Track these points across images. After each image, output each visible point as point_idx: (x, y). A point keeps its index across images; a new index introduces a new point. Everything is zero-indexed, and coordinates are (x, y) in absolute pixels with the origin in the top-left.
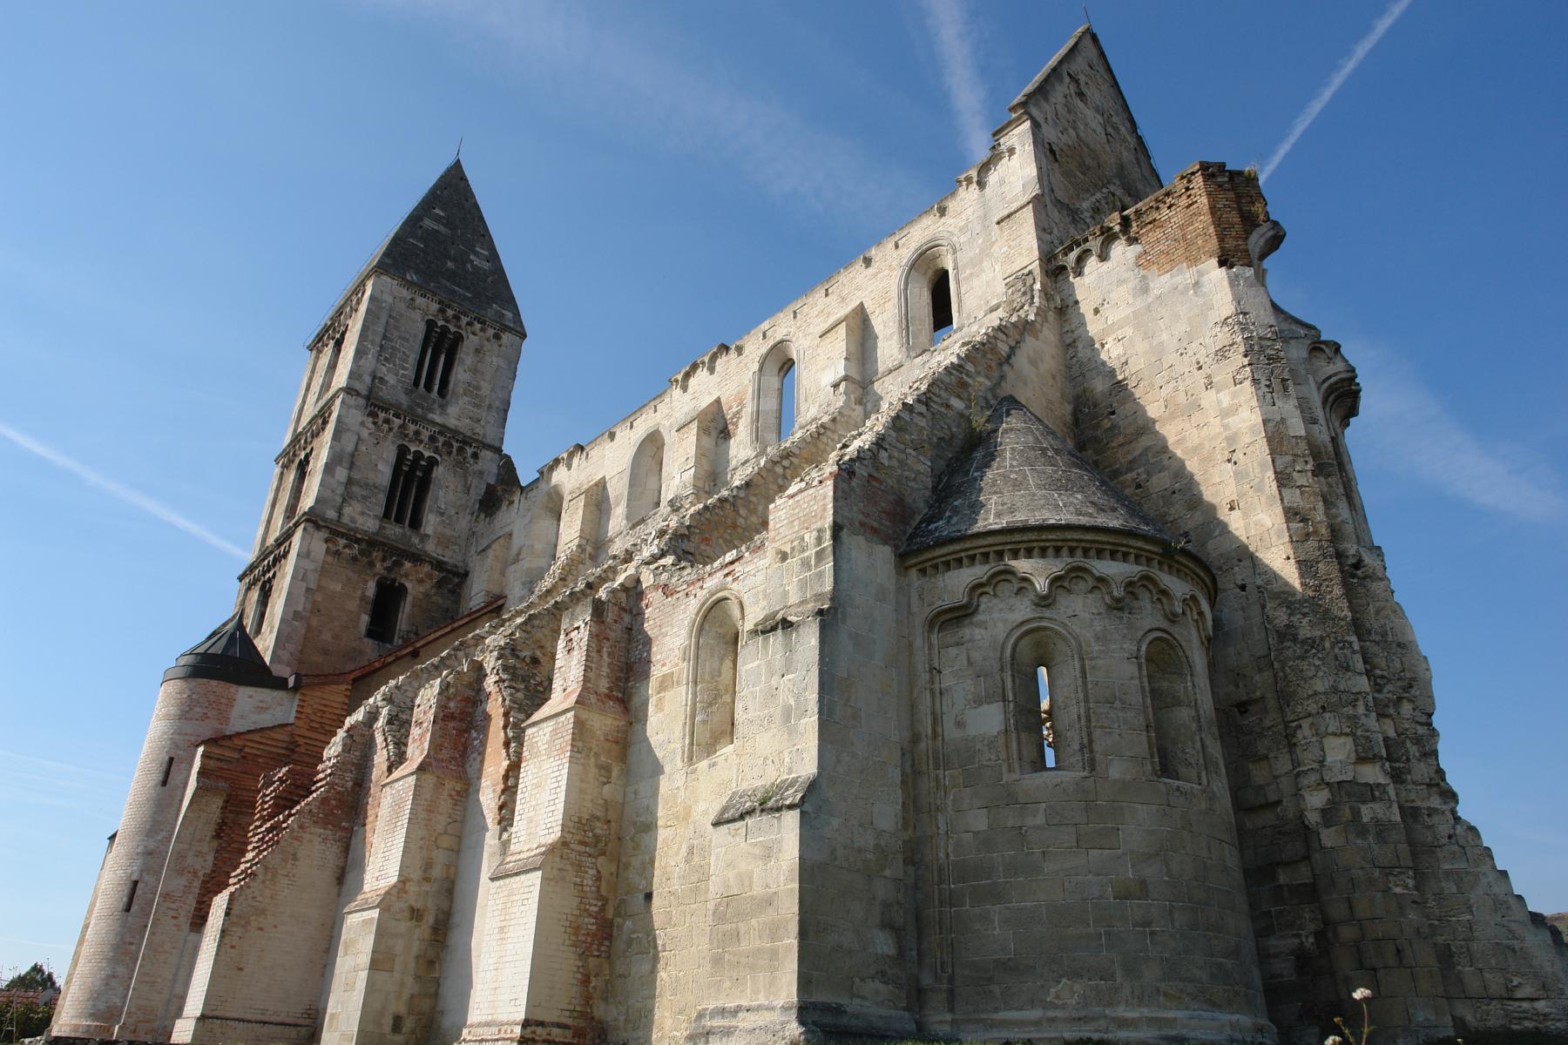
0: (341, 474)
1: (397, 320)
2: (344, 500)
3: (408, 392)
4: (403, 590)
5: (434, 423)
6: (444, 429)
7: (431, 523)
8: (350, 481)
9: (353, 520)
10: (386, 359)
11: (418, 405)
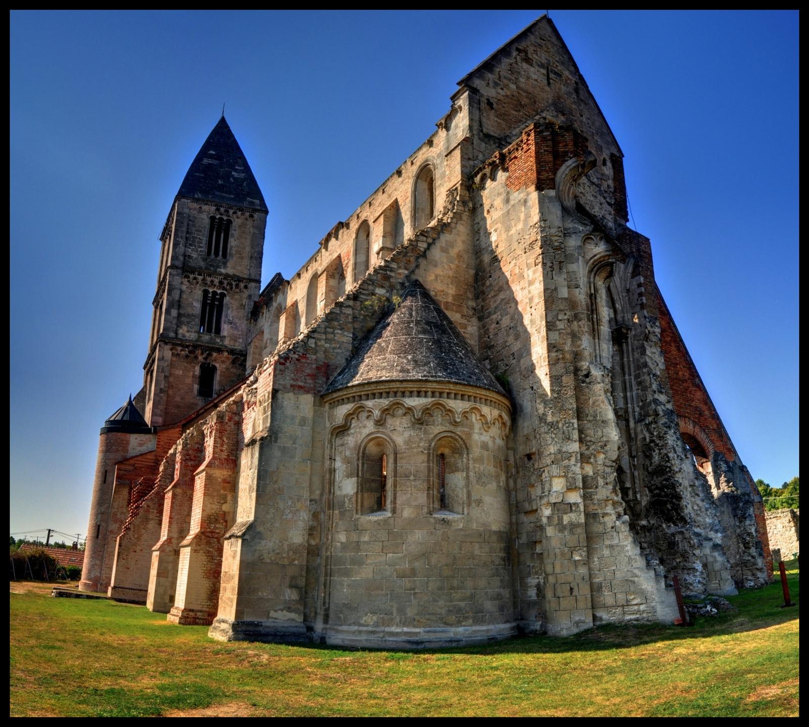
0: (174, 312)
1: (193, 222)
2: (178, 326)
3: (204, 260)
4: (214, 368)
5: (221, 274)
6: (227, 276)
7: (226, 329)
8: (179, 315)
9: (184, 336)
10: (190, 245)
11: (211, 266)
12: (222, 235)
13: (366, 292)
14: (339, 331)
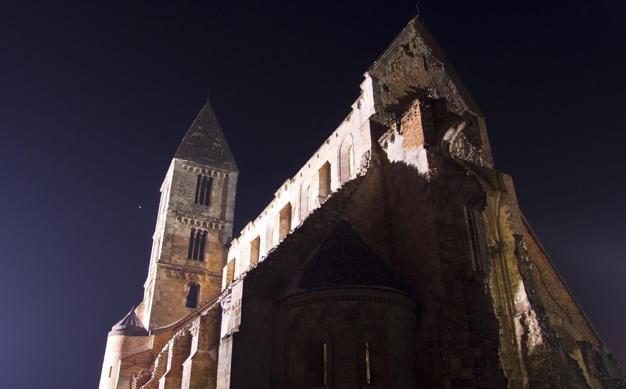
0: (169, 244)
2: (171, 255)
3: (192, 206)
4: (199, 286)
5: (204, 217)
7: (207, 257)
8: (173, 247)
9: (176, 262)
10: (183, 195)
11: (198, 211)
12: (206, 189)
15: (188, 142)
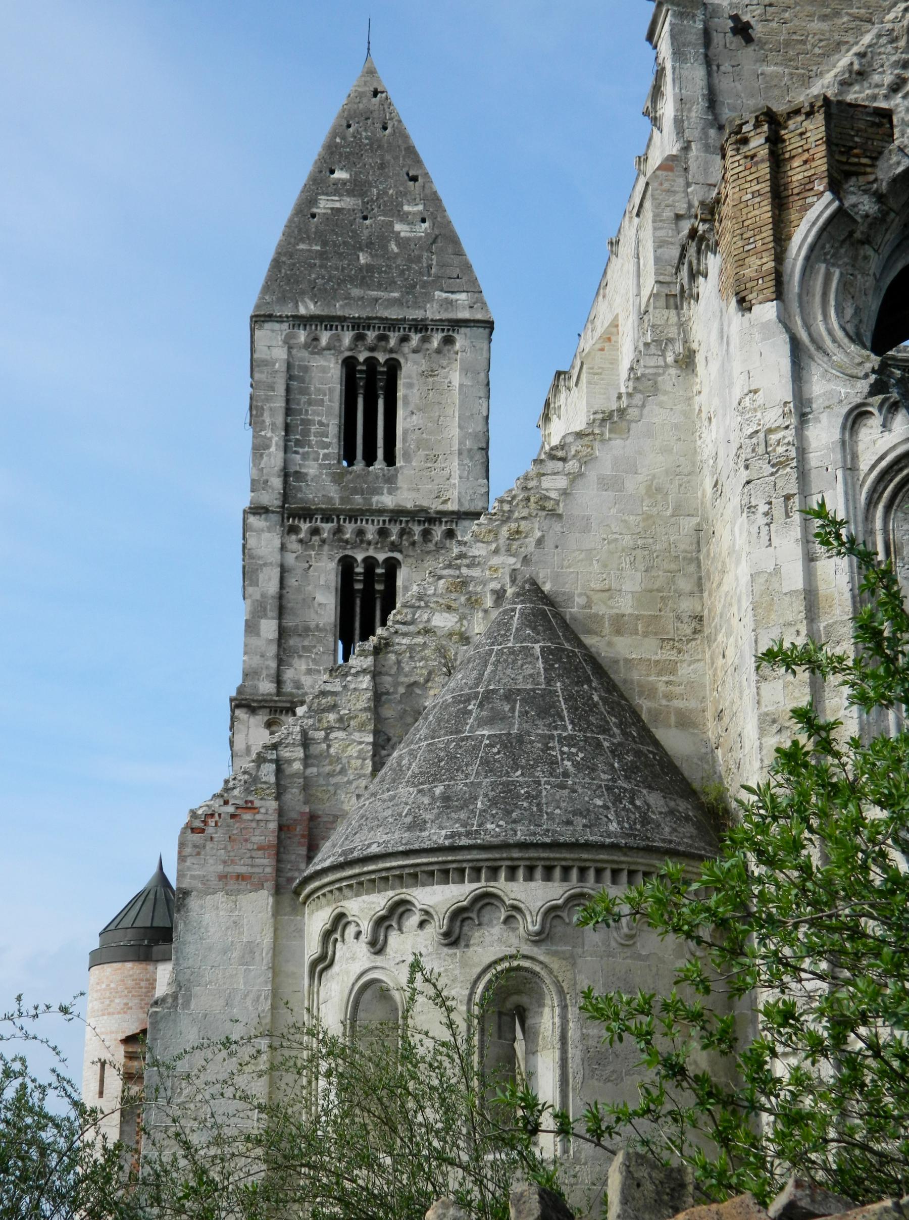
1: (302, 380)
3: (338, 478)
5: (381, 512)
6: (397, 514)
10: (298, 443)
11: (355, 491)
13: (412, 628)
14: (341, 734)
15: (302, 240)
